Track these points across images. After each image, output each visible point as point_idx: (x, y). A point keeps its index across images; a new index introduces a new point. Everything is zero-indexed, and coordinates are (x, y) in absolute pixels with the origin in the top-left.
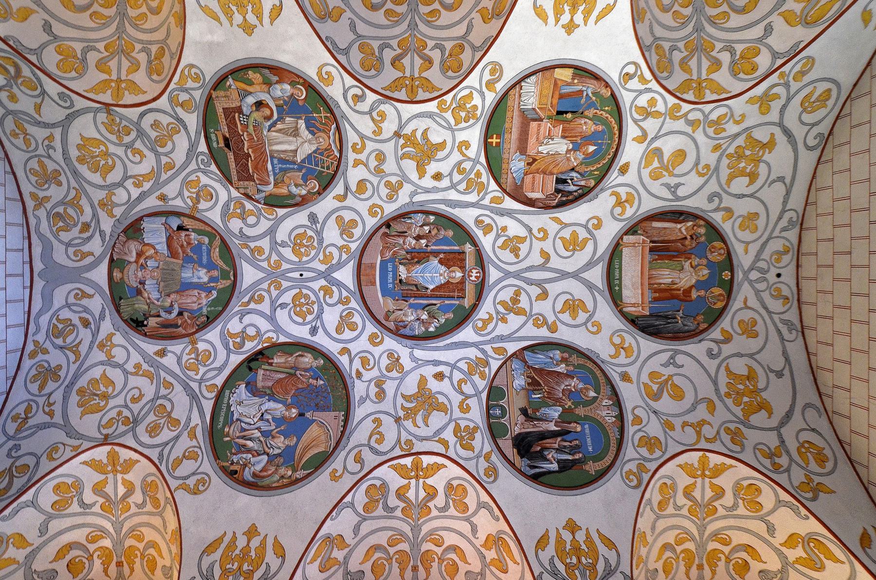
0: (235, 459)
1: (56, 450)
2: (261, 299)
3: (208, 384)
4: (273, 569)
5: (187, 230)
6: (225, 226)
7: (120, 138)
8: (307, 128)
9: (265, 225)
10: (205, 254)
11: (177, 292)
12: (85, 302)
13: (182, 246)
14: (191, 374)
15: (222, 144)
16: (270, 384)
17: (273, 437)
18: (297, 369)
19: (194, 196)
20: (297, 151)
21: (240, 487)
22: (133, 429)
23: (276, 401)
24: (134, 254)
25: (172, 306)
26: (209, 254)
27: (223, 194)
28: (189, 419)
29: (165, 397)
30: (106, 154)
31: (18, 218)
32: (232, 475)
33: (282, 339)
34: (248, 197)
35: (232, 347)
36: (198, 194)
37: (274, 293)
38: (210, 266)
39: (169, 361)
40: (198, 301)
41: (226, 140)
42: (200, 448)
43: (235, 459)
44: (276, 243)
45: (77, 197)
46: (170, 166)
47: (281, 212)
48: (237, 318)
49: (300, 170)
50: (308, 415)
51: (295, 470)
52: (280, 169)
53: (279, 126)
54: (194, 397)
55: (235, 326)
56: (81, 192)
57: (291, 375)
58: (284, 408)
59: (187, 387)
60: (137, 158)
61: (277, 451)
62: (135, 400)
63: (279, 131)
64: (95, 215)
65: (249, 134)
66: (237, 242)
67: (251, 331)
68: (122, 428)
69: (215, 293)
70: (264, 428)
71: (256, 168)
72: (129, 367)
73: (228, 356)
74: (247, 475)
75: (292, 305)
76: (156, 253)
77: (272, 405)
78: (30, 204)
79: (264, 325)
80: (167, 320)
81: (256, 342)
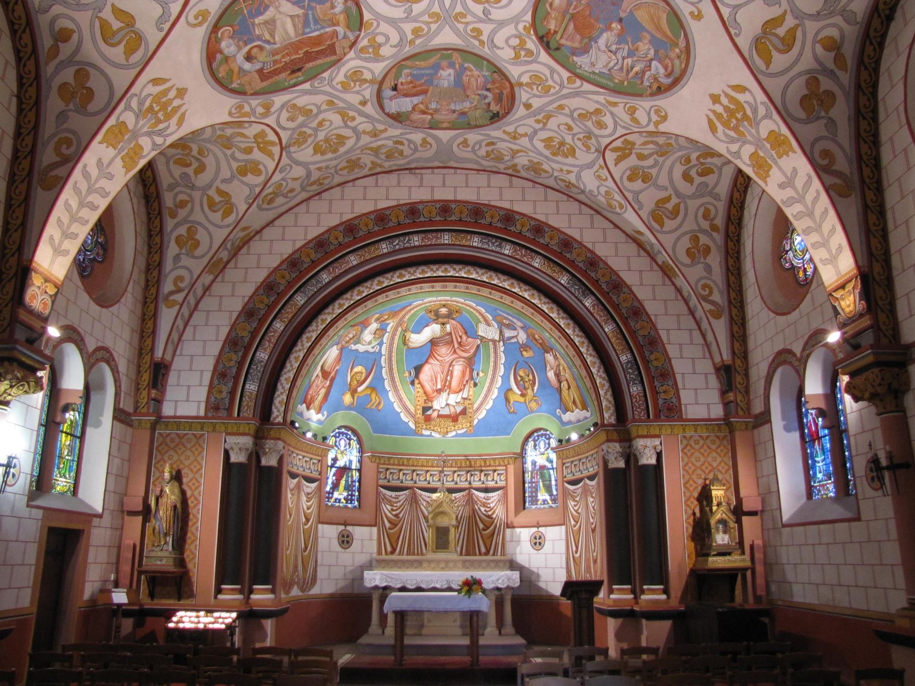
0: (646, 83)
1: (599, 177)
2: (479, 32)
3: (566, 82)
4: (751, 100)
5: (396, 85)
6: (388, 58)
7: (310, 136)
8: (261, 14)
9: (384, 27)
10: (423, 72)
11: (465, 91)
12: (471, 143)
13: (414, 87)
14: (552, 91)
15: (300, 74)
16: (578, 37)
17: (637, 50)
18: (564, 14)
19: (358, 83)
20: (291, 16)
21: (674, 90)
22: (596, 137)
23: (599, 37)
24: (424, 116)
25: (479, 95)
26: (422, 69)
27: (352, 62)
28: (598, 102)
29: (572, 112)
30: (327, 140)
31: (393, 177)
32: (660, 90)
33: (528, 17)
34: (354, 43)
35: (530, 59)
36: (355, 82)
37: (469, 18)
38: (437, 67)
39: (536, 103)
40: (476, 76)
41: (293, 72)
42: (627, 103)
43: (646, 83)
44: (407, 18)
45: (371, 149)
46: (330, 103)
47: (367, 16)
48: (498, 52)
49: (313, 9)
50: (622, 15)
51: (676, 45)
52: (315, 24)
53: (268, 37)
54: (577, 94)
55: (506, 54)
56: (366, 147)
57: (573, 17)
58: (609, 33)
59: (565, 97)
60: (328, 123)
61: (652, 52)
62: (570, 128)
63: (273, 36)
64: (385, 139)
65: (283, 57)
66: (407, 48)
67: (515, 42)
68: (593, 141)
69: (466, 65)
70: (625, 54)
71: (319, 44)
72: (537, 126)
73: (540, 63)
74: (667, 81)
75: (486, 5)
76: (422, 103)
77: (602, 42)
78: (378, 170)
79: (509, 30)
80: (494, 99)
81: (527, 40)
